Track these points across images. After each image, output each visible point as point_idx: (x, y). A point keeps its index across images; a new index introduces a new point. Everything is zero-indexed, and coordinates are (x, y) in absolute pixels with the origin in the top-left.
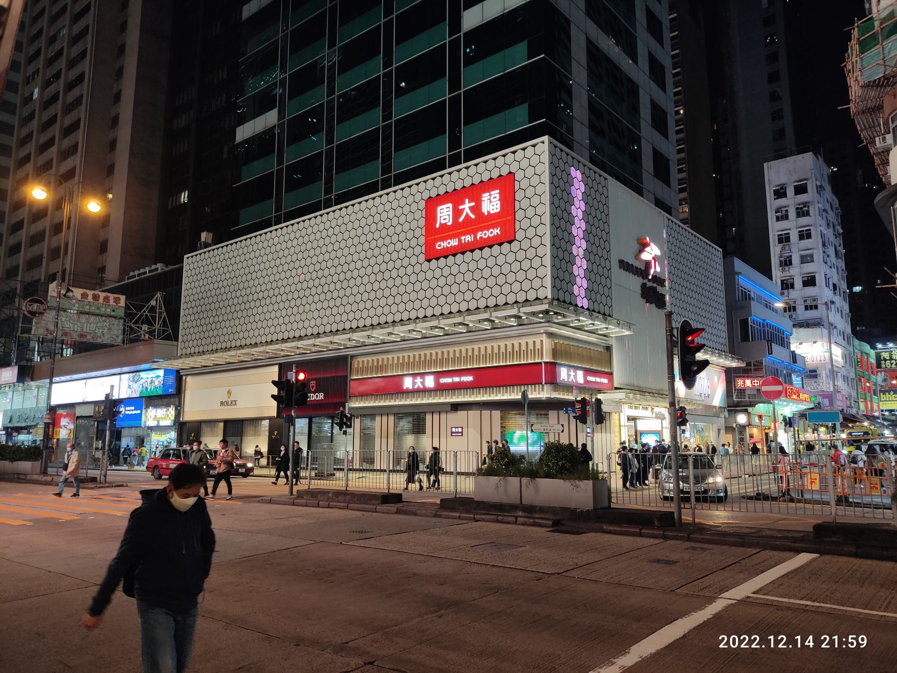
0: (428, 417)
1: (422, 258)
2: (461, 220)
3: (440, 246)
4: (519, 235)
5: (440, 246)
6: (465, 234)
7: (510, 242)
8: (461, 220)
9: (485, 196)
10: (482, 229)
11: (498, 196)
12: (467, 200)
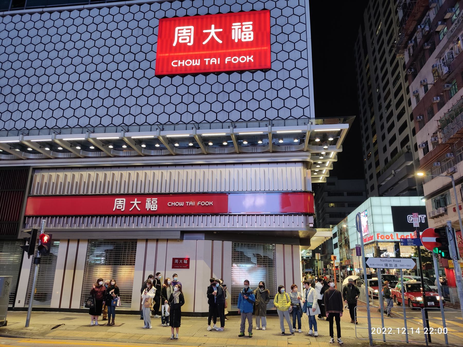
0: (140, 246)
1: (151, 73)
2: (204, 43)
3: (176, 63)
4: (276, 66)
5: (176, 63)
6: (210, 57)
7: (265, 71)
8: (204, 43)
9: (236, 26)
10: (232, 55)
11: (251, 27)
12: (213, 26)
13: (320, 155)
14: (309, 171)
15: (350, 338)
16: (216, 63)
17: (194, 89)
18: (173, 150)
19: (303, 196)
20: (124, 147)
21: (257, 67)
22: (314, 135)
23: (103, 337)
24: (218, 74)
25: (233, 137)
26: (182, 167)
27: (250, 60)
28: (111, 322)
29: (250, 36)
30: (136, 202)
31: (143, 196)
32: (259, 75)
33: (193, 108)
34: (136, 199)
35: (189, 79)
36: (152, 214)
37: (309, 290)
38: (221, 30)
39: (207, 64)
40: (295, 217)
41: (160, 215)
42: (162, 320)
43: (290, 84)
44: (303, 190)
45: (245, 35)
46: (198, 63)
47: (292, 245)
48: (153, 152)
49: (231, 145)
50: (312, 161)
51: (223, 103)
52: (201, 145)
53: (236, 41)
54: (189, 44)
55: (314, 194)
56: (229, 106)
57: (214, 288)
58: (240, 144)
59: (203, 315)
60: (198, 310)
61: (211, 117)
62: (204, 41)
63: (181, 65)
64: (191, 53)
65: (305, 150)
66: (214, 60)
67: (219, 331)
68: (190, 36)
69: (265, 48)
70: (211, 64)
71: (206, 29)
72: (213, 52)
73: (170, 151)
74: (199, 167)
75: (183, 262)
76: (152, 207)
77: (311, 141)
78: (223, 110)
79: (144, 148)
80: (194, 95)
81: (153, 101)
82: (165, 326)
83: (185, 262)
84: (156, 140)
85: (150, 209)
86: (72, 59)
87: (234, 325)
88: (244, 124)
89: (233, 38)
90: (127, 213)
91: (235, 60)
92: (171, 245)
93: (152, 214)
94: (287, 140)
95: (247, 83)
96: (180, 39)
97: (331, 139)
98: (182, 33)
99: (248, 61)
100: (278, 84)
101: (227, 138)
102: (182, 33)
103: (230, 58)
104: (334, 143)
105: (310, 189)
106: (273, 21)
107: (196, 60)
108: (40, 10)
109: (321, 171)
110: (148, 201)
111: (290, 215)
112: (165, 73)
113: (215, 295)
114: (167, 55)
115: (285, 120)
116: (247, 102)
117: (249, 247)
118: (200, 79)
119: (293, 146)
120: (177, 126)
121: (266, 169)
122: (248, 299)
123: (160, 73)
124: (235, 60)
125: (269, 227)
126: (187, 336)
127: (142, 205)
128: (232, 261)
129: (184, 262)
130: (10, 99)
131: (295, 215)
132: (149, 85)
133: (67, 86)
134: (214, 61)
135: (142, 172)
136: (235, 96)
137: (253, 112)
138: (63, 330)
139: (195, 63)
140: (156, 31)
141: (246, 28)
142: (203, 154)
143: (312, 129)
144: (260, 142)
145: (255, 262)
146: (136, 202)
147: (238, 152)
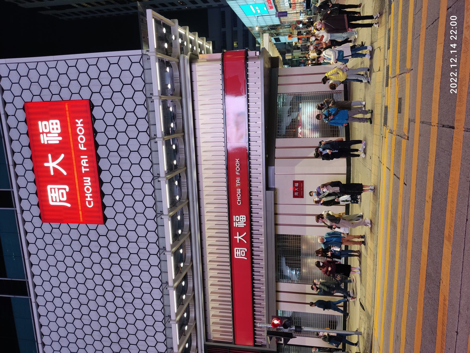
0: (282, 231)
1: (102, 229)
2: (65, 173)
3: (90, 202)
4: (86, 94)
5: (90, 202)
6: (80, 166)
7: (92, 106)
8: (65, 173)
9: (44, 139)
10: (76, 143)
11: (44, 123)
12: (46, 164)
13: (182, 44)
14: (200, 56)
15: (373, 7)
16: (87, 160)
17: (117, 183)
18: (183, 202)
19: (226, 62)
20: (181, 251)
21: (89, 115)
22: (160, 48)
23: (372, 259)
24: (98, 158)
25: (167, 138)
26: (201, 192)
27: (81, 123)
28: (357, 254)
29: (54, 124)
30: (238, 237)
31: (232, 230)
32: (97, 113)
33: (137, 183)
34: (235, 237)
35: (106, 189)
36: (250, 221)
37: (325, 57)
38: (50, 156)
39: (88, 170)
40: (249, 71)
41: (251, 212)
42: (354, 203)
43: (105, 78)
44: (220, 62)
45: (53, 129)
46: (87, 180)
47: (279, 76)
48: (186, 223)
49: (176, 141)
50: (190, 53)
51: (131, 151)
52: (177, 173)
53: (60, 138)
54: (68, 190)
55: (225, 51)
56: (134, 145)
57: (324, 153)
58: (174, 132)
59: (349, 164)
60: (344, 169)
61: (146, 164)
62: (62, 174)
63: (91, 197)
64: (77, 187)
65: (177, 60)
66: (83, 162)
67: (366, 145)
68: (59, 189)
69: (67, 106)
70: (87, 165)
71: (49, 171)
72: (74, 164)
73: (184, 205)
74: (199, 158)
75: (297, 187)
76: (243, 221)
77: (168, 52)
78: (137, 151)
79: (182, 231)
80: (124, 183)
81: (131, 225)
82: (361, 200)
83: (297, 185)
84: (173, 218)
85: (245, 223)
86: (67, 267)
87: (359, 130)
88: (152, 127)
89: (58, 142)
90: (249, 245)
91: (82, 139)
92: (280, 200)
93: (250, 221)
94: (168, 80)
95: (107, 126)
96: (62, 199)
97: (164, 30)
98: (56, 197)
99: (82, 125)
100: (106, 92)
101: (168, 144)
102: (56, 197)
103: (80, 145)
104: (169, 28)
105: (219, 55)
106: (37, 99)
107: (85, 181)
108: (40, 346)
109: (200, 45)
110: (237, 224)
111: (247, 76)
112: (101, 214)
113: (331, 151)
114: (80, 212)
115: (145, 84)
116: (128, 125)
117: (280, 121)
118: (105, 176)
119: (174, 74)
120: (158, 199)
121: (198, 83)
122: (334, 115)
123: (102, 219)
124: (82, 139)
125: (260, 99)
126: (371, 176)
127: (241, 231)
128: (296, 137)
129: (297, 186)
130: (124, 344)
131: (247, 71)
132: (115, 230)
133: (121, 313)
134: (84, 163)
135: (207, 233)
136: (122, 139)
137: (138, 118)
138: (365, 300)
139: (88, 183)
140: (55, 225)
141: (46, 128)
142: (186, 171)
143: (154, 50)
144: (171, 109)
145: (297, 114)
146: (238, 237)
147: (182, 134)
